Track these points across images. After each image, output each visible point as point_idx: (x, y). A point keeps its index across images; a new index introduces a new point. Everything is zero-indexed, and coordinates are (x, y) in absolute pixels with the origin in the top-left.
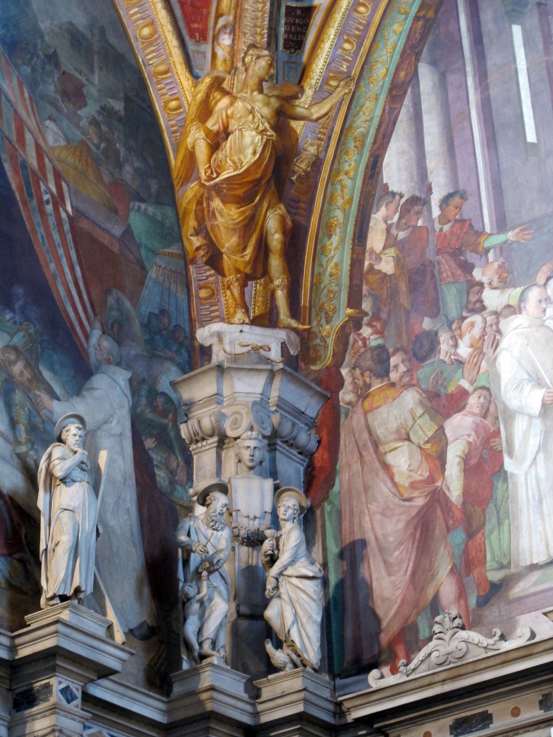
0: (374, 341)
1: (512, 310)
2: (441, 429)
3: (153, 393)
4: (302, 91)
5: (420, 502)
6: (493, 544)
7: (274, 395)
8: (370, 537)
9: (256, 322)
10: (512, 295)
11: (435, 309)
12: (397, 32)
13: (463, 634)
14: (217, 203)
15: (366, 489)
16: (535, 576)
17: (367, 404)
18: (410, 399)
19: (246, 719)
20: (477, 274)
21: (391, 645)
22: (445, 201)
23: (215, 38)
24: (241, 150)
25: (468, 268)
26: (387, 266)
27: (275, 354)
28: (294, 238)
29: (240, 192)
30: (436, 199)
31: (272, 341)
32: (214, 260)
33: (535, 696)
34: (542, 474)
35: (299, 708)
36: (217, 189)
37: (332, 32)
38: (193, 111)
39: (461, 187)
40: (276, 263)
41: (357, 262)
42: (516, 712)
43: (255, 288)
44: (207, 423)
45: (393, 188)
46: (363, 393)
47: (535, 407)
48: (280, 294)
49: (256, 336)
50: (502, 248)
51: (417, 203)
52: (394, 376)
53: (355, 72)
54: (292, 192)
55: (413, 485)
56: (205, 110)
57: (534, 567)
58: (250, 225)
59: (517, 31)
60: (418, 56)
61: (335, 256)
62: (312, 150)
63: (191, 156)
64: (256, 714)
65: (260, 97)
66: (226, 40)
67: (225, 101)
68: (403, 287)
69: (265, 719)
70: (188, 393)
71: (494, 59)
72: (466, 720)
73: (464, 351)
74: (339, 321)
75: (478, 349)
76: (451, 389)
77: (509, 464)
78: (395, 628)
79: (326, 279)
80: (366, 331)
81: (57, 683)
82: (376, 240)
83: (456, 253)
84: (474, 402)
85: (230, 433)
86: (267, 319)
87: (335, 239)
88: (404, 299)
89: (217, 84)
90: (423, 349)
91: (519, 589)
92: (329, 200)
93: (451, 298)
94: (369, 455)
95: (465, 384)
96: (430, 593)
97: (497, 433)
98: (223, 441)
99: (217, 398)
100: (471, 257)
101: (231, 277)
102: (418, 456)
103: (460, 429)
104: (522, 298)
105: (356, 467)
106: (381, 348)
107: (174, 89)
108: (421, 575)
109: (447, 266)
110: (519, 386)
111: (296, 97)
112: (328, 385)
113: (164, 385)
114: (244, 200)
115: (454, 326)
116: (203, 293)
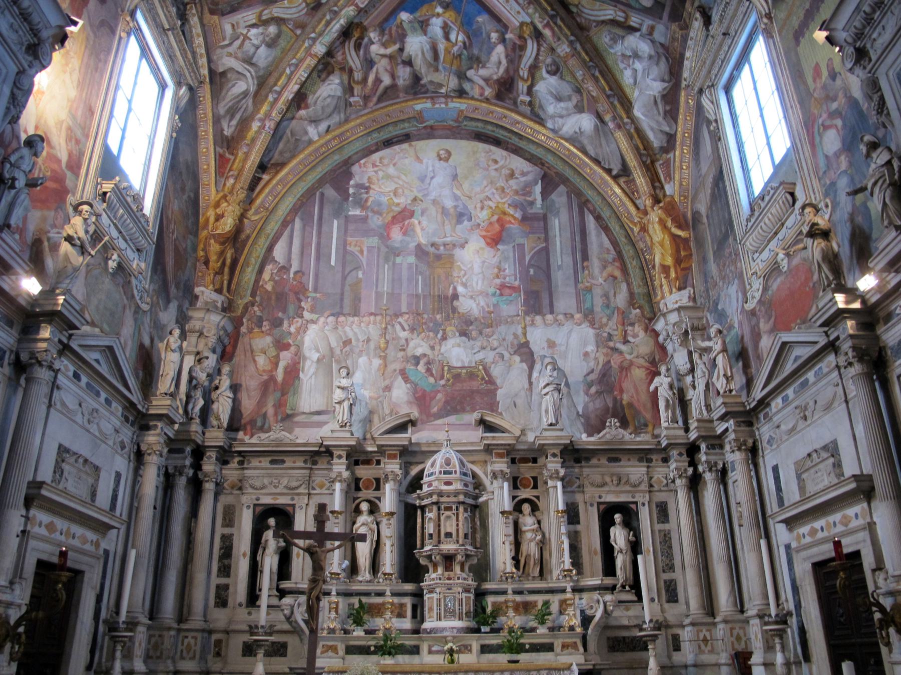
0: (258, 313)
1: (314, 322)
2: (278, 354)
3: (182, 311)
4: (251, 208)
5: (266, 377)
6: (290, 400)
7: (222, 324)
8: (244, 384)
9: (216, 291)
10: (314, 317)
11: (284, 311)
12: (289, 202)
13: (283, 433)
14: (212, 241)
15: (245, 366)
16: (304, 416)
17: (251, 335)
18: (269, 339)
19: (200, 442)
20: (303, 304)
21: (245, 425)
22: (296, 273)
23: (227, 178)
24: (225, 224)
25: (300, 301)
26: (269, 287)
27: (219, 305)
28: (235, 262)
29: (222, 240)
30: (293, 270)
31: (219, 299)
32: (207, 263)
33: (303, 458)
34: (313, 383)
35: (221, 444)
36: (214, 236)
37: (267, 191)
38: (213, 203)
39: (303, 269)
40: (226, 270)
41: (257, 281)
42: (294, 462)
43: (218, 277)
44: (197, 328)
45: (277, 259)
46: (250, 331)
47: (315, 359)
48: (226, 282)
49: (215, 296)
50: (314, 299)
51: (285, 269)
52: (264, 329)
53: (270, 208)
54: (238, 245)
55: (264, 371)
56: (217, 205)
57: (304, 413)
58: (222, 253)
59: (336, 222)
60: (296, 213)
61: (249, 275)
62: (248, 232)
63: (207, 220)
64: (203, 442)
65: (238, 207)
66: (232, 181)
67: (225, 204)
68: (274, 298)
69: (206, 444)
70: (190, 313)
71: (325, 228)
72: (276, 460)
73: (292, 329)
74: (246, 301)
75: (298, 330)
76: (285, 341)
77: (301, 375)
78: (248, 419)
79: (243, 283)
80: (256, 308)
81: (160, 424)
82: (266, 276)
83: (296, 293)
84: (293, 349)
85: (205, 334)
86: (219, 291)
87: (250, 269)
88: (273, 302)
89: (224, 197)
90: (277, 323)
91: (297, 419)
92: (250, 252)
93: (291, 309)
94: (249, 354)
95: (290, 341)
96: (264, 411)
97: (299, 363)
98: (201, 334)
99: (203, 319)
100: (302, 297)
101: (211, 271)
102: (268, 361)
103: (286, 357)
104: (318, 319)
105: (243, 357)
106: (261, 317)
107: (209, 192)
108: (261, 403)
109: (292, 297)
110: (310, 350)
111: (248, 210)
112: (237, 323)
113: (185, 310)
114: (222, 244)
115: (291, 319)
116: (200, 274)
